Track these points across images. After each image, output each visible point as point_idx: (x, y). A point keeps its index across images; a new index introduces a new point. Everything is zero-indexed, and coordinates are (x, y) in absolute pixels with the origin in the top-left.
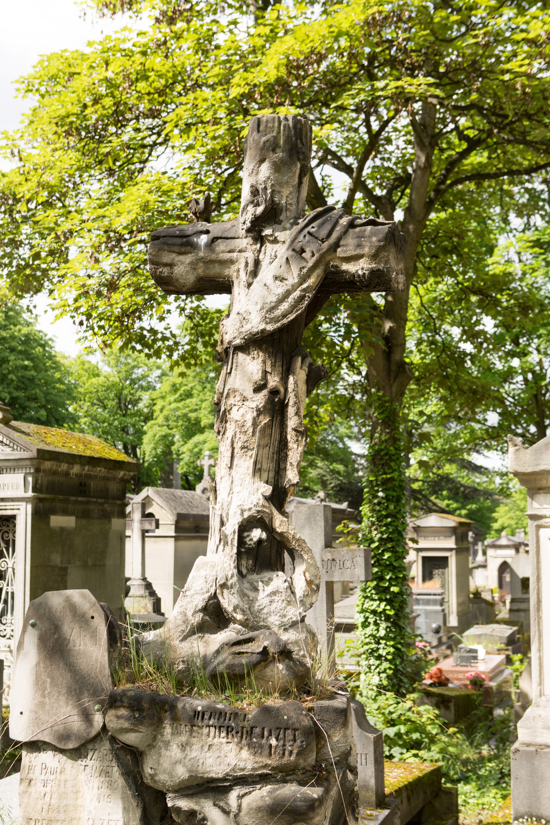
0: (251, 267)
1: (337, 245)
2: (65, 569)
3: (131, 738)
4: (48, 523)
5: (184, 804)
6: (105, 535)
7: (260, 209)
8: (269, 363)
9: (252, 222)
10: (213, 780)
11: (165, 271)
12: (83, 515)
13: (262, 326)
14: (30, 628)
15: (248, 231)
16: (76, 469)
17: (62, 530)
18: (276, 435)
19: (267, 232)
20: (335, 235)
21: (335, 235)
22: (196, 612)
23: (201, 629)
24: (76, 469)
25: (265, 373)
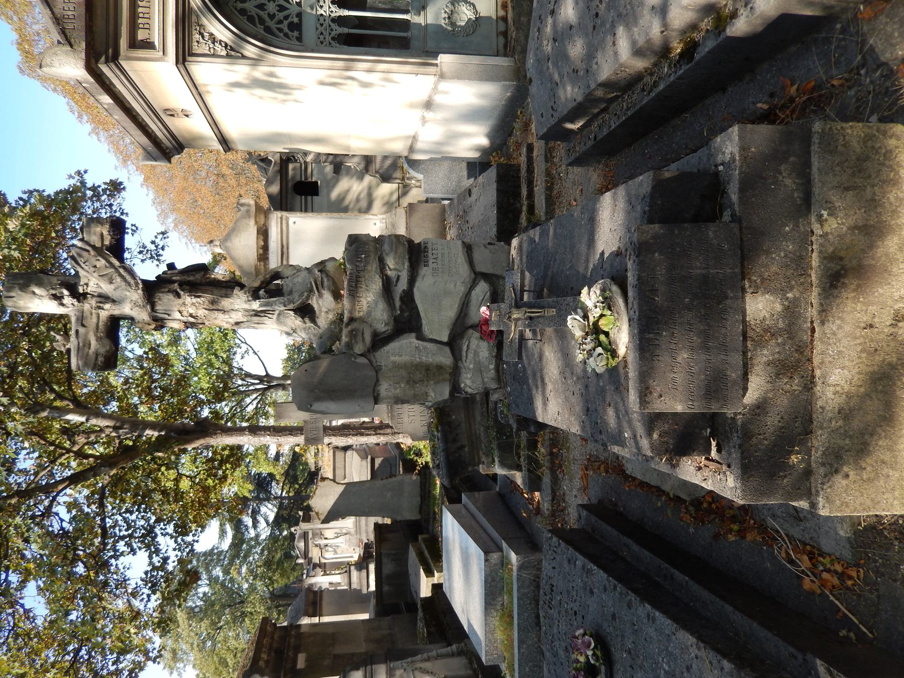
0: (102, 300)
1: (94, 247)
2: (336, 657)
3: (368, 338)
4: (301, 670)
5: (398, 303)
6: (311, 635)
7: (66, 292)
8: (163, 290)
9: (74, 298)
10: (383, 285)
11: (101, 359)
12: (297, 650)
13: (140, 292)
14: (313, 408)
15: (79, 301)
16: (264, 656)
17: (307, 661)
18: (207, 288)
19: (81, 290)
20: (88, 248)
21: (88, 248)
22: (305, 323)
23: (313, 320)
24: (264, 656)
25: (169, 292)
